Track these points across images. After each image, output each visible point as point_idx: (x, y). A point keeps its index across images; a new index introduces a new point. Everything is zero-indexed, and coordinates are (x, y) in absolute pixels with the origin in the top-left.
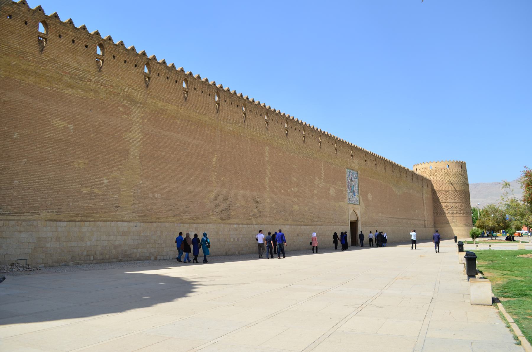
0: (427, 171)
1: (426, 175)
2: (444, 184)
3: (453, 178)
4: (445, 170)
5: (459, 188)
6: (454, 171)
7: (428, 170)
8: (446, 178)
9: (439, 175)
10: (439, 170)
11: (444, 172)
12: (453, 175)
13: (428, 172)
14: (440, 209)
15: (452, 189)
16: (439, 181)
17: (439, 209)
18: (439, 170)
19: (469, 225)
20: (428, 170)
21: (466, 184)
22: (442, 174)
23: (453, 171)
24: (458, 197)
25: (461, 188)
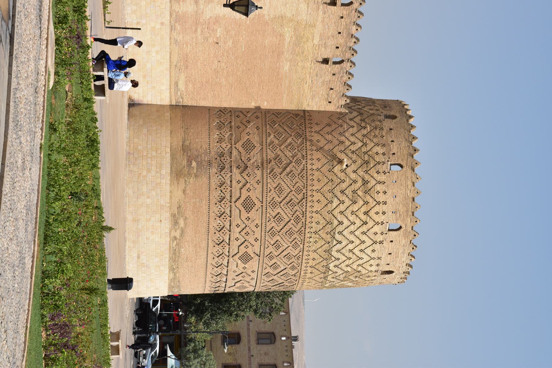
0: (376, 108)
1: (363, 105)
3: (355, 182)
4: (381, 156)
5: (315, 199)
6: (379, 187)
8: (354, 157)
9: (364, 136)
12: (365, 182)
14: (238, 127)
15: (312, 170)
17: (240, 125)
19: (177, 234)
20: (381, 110)
23: (380, 183)
24: (281, 191)
25: (314, 210)
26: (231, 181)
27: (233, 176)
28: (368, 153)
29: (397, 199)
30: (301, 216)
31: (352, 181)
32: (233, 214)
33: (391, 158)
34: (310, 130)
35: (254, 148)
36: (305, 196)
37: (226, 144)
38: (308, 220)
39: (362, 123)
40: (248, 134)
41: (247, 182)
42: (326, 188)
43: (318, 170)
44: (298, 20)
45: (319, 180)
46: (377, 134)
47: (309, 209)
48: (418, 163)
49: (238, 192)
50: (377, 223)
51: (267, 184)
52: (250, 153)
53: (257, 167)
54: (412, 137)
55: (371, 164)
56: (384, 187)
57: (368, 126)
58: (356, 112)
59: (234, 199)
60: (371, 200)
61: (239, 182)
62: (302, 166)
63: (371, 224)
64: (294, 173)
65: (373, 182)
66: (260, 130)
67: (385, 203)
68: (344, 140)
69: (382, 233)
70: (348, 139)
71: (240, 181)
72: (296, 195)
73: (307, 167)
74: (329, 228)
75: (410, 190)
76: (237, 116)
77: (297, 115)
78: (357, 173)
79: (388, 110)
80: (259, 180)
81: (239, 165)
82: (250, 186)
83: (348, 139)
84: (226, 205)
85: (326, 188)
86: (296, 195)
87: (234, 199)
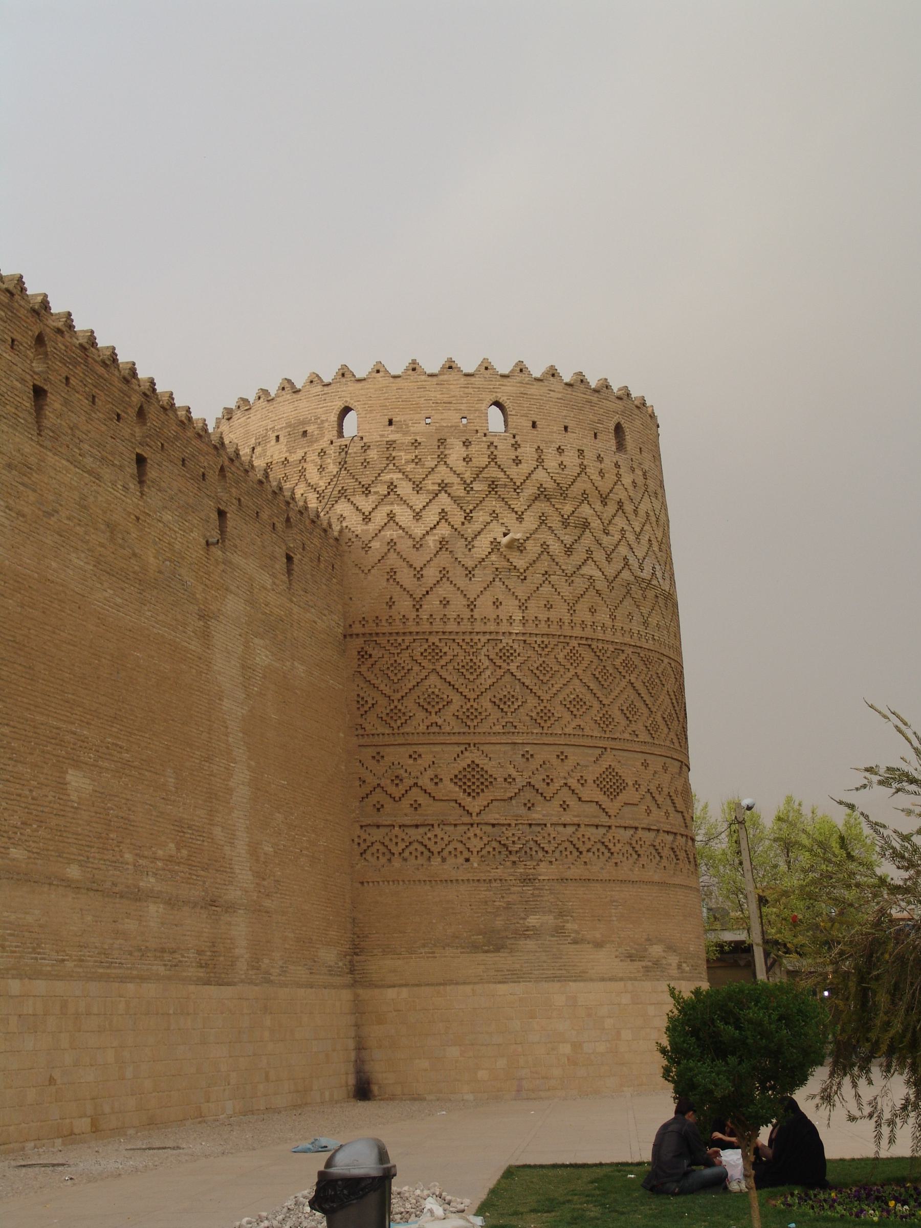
0: (313, 457)
2: (457, 574)
3: (543, 520)
4: (473, 449)
5: (588, 618)
6: (552, 463)
7: (324, 443)
8: (481, 517)
9: (418, 488)
10: (416, 444)
11: (460, 466)
12: (542, 495)
13: (322, 468)
14: (416, 806)
15: (524, 621)
16: (418, 545)
17: (405, 803)
18: (416, 444)
19: (673, 960)
21: (650, 594)
22: (443, 487)
23: (540, 461)
25: (609, 623)
26: (565, 825)
27: (555, 820)
28: (468, 482)
29: (571, 425)
30: (623, 656)
31: (544, 526)
32: (631, 822)
33: (477, 428)
34: (410, 623)
35: (478, 765)
36: (584, 642)
37: (473, 839)
38: (627, 640)
39: (376, 493)
40: (437, 780)
41: (566, 784)
42: (565, 590)
43: (523, 607)
44: (246, 623)
45: (549, 607)
46: (411, 456)
47: (609, 636)
48: (486, 365)
49: (586, 807)
50: (618, 475)
51: (565, 734)
52: (491, 776)
53: (528, 759)
54: (410, 372)
55: (498, 476)
56: (550, 451)
57: (386, 477)
58: (336, 506)
59: (604, 820)
60: (580, 486)
61: (565, 807)
62: (516, 646)
63: (620, 494)
64: (536, 666)
65: (540, 475)
66: (421, 749)
67: (581, 452)
68: (437, 538)
69: (633, 470)
70: (431, 529)
71: (562, 803)
72: (585, 664)
73: (517, 634)
74: (636, 592)
75: (550, 390)
76: (378, 810)
77: (363, 655)
78: (522, 513)
79: (320, 428)
80: (558, 756)
81: (525, 804)
82: (573, 778)
83: (431, 529)
84: (617, 838)
85: (565, 590)
86: (585, 664)
87: (604, 820)
